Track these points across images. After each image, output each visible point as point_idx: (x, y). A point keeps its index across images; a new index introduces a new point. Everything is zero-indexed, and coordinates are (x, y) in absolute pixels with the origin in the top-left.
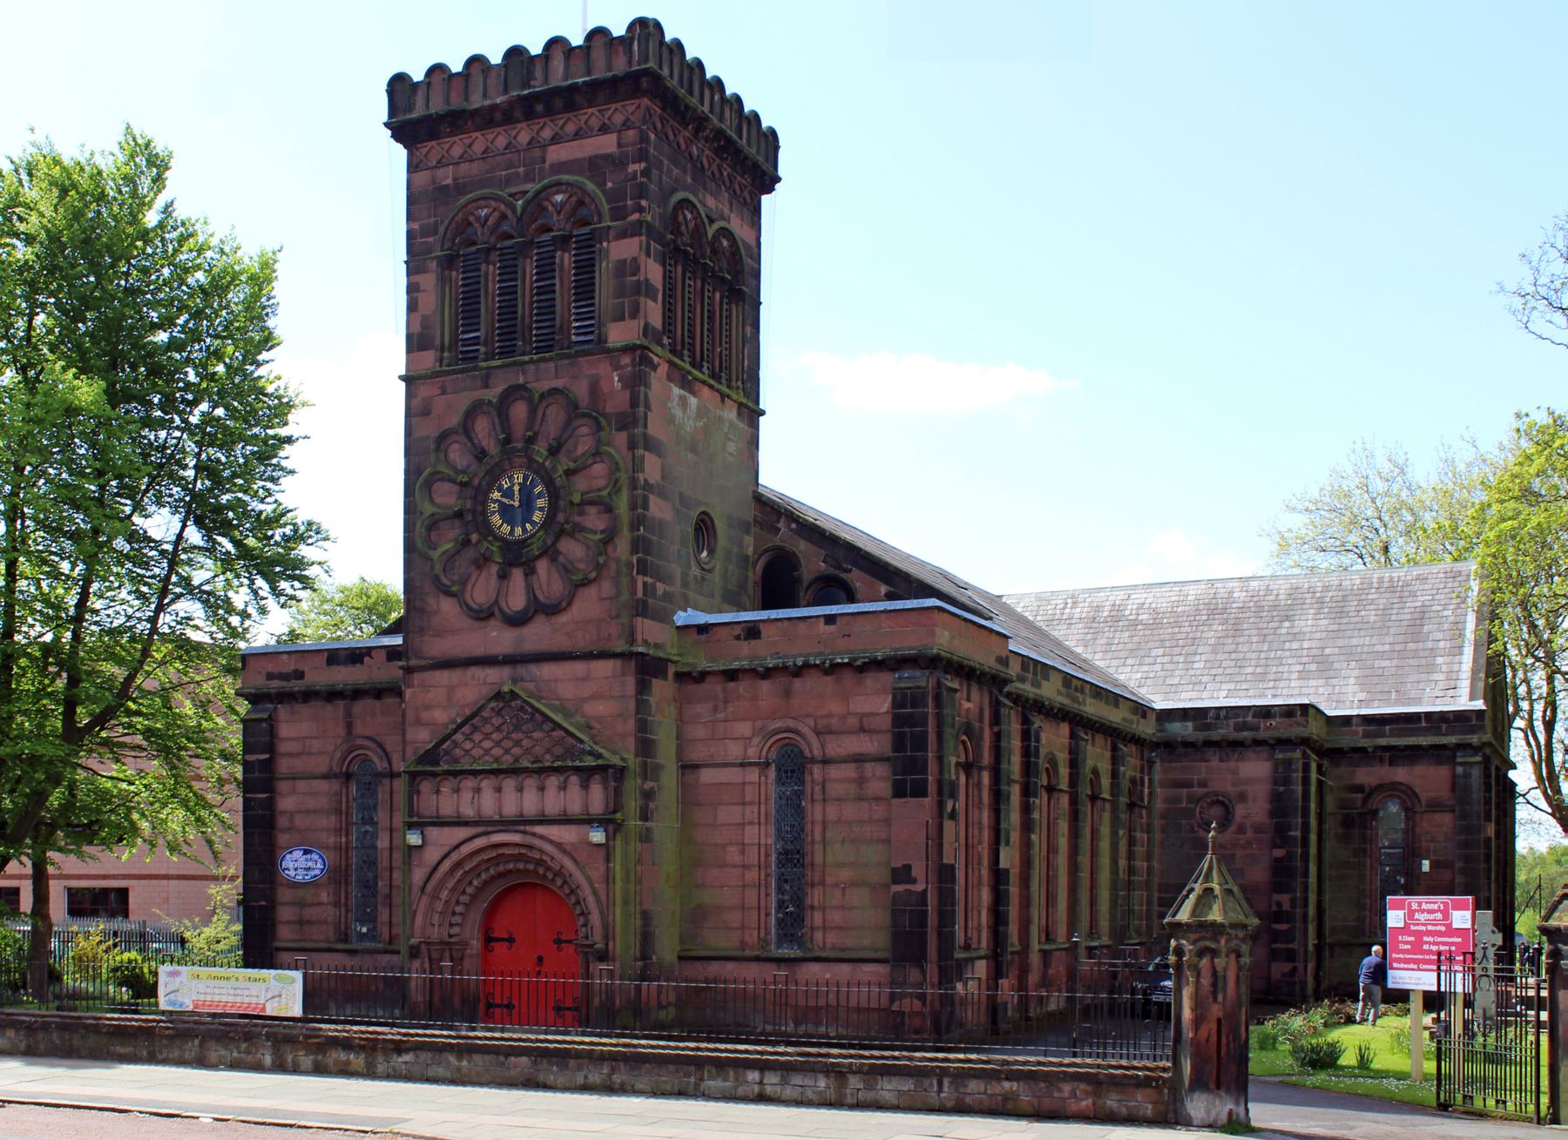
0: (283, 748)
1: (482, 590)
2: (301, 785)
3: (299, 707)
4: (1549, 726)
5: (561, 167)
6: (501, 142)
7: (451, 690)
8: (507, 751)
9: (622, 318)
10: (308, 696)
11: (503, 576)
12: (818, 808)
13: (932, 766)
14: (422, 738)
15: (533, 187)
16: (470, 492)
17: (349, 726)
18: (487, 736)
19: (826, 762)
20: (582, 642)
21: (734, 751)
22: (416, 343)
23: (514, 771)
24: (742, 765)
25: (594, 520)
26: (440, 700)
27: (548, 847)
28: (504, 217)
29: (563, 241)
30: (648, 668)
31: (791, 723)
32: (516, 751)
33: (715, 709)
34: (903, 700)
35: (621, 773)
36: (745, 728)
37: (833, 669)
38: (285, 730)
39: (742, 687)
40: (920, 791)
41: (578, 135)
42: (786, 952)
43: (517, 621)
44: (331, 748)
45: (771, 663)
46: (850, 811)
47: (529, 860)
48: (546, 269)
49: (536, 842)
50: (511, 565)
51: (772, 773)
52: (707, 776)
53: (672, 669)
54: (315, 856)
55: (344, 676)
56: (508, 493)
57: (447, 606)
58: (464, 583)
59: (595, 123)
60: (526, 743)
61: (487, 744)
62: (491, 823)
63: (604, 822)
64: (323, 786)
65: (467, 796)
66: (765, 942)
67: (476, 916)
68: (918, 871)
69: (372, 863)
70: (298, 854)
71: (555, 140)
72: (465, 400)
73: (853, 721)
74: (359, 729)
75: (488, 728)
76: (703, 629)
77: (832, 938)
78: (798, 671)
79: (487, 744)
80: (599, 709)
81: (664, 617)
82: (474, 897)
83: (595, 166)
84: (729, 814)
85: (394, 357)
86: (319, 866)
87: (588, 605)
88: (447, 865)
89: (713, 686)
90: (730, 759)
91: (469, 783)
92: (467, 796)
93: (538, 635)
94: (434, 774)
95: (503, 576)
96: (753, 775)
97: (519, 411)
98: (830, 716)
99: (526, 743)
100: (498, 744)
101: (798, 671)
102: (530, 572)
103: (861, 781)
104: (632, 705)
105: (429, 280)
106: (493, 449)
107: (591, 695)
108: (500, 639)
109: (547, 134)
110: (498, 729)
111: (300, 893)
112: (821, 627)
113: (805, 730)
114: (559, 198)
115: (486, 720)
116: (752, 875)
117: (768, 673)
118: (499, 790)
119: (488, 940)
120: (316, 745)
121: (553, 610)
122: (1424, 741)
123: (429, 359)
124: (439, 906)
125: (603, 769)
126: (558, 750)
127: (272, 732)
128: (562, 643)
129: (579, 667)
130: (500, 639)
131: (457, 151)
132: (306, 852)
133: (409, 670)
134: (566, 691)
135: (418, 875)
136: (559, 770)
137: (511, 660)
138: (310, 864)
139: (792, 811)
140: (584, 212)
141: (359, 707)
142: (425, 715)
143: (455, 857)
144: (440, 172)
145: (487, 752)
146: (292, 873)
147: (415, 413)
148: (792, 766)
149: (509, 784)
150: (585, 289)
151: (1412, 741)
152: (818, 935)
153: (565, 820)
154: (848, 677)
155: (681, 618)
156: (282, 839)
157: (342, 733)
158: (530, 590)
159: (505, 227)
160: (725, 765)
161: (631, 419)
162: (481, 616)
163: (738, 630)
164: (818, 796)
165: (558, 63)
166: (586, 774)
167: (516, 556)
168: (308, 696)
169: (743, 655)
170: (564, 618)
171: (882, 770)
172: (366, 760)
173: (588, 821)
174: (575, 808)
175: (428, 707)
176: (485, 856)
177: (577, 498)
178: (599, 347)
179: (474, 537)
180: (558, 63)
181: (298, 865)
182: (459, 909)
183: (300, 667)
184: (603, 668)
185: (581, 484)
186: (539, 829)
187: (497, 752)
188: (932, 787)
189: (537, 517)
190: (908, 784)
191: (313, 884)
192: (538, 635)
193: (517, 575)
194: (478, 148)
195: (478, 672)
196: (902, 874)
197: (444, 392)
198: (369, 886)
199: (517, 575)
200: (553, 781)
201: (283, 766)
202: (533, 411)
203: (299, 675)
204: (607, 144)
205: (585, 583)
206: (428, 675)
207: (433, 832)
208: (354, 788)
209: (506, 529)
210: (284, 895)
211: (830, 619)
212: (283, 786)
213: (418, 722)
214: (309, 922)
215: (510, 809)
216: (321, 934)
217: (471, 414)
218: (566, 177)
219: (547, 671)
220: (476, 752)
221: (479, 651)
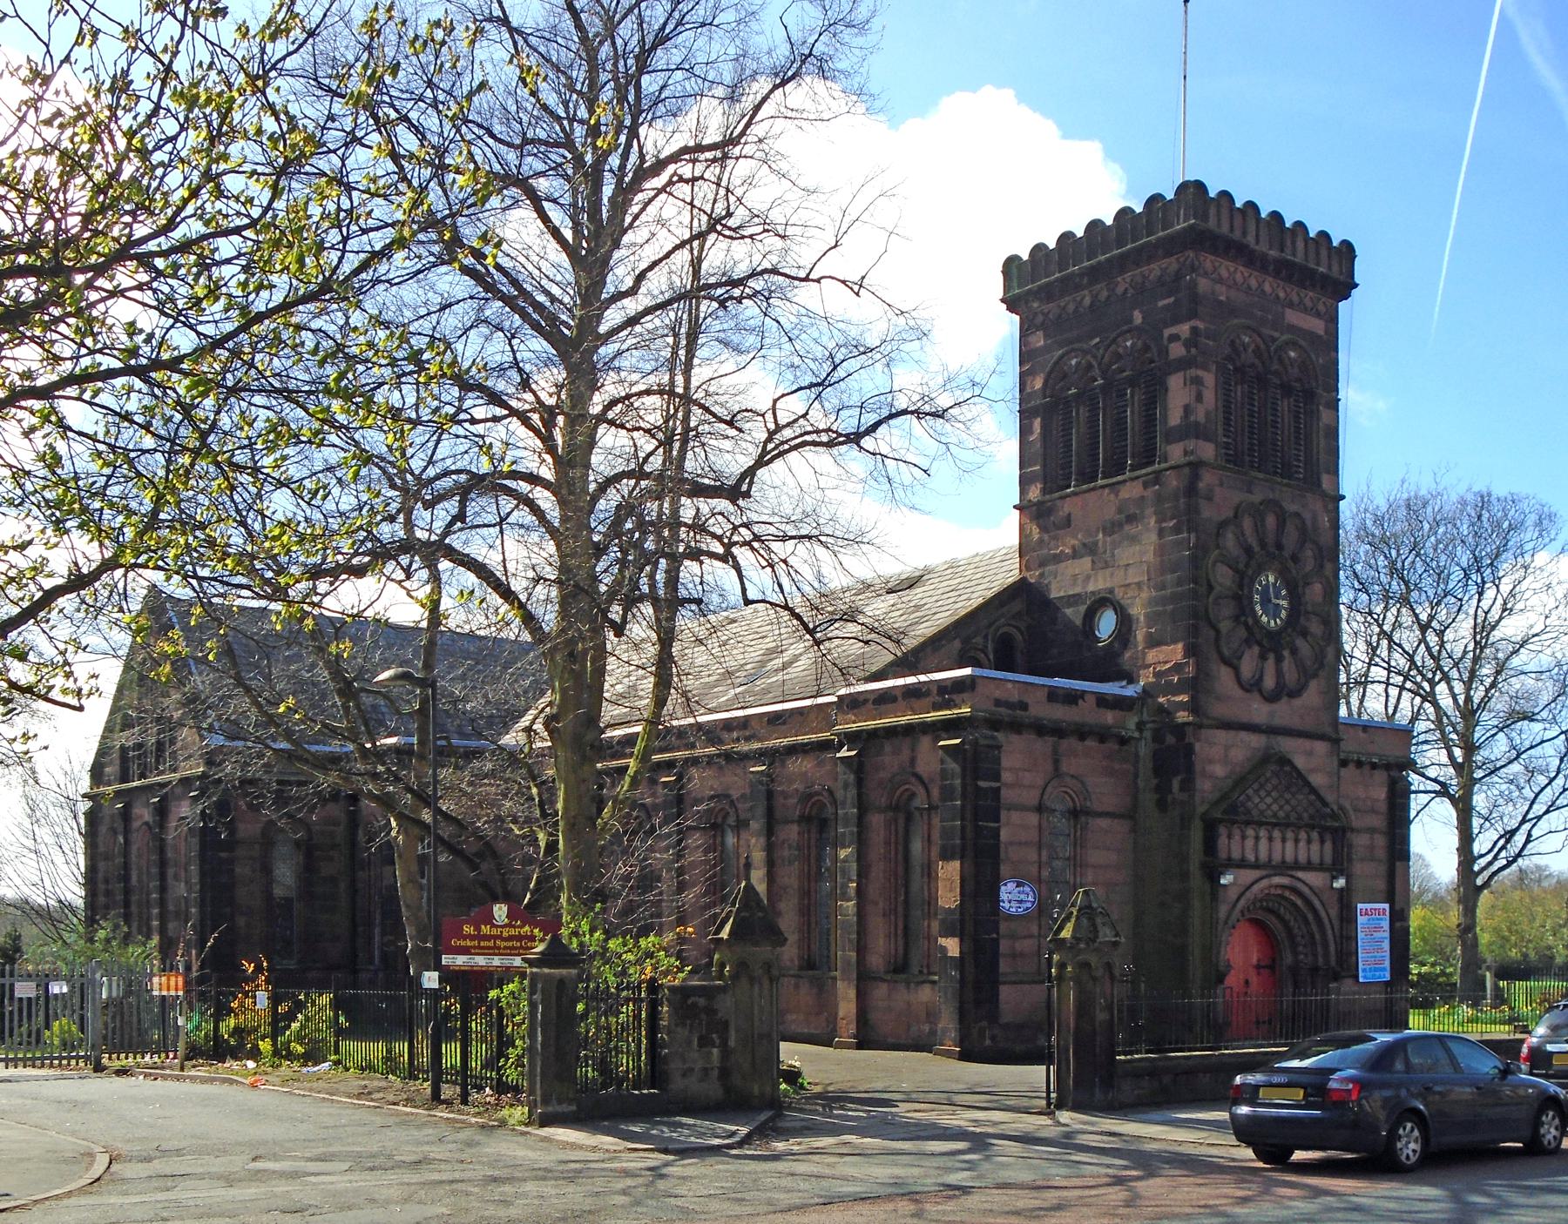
7: (1227, 748)
8: (1281, 807)
17: (1056, 762)
18: (1269, 794)
20: (1308, 724)
23: (1283, 825)
32: (1287, 808)
43: (1272, 698)
44: (1040, 782)
50: (1270, 650)
54: (1027, 889)
57: (1225, 673)
60: (1293, 802)
61: (1269, 800)
70: (1011, 886)
72: (1237, 497)
74: (1064, 768)
87: (1312, 695)
93: (1283, 714)
99: (1293, 802)
100: (1275, 801)
108: (1259, 711)
110: (1275, 788)
114: (1292, 354)
120: (1028, 778)
121: (1294, 694)
130: (1259, 711)
137: (1272, 731)
138: (1022, 897)
141: (1065, 744)
142: (1209, 768)
144: (1218, 287)
145: (1269, 806)
146: (1007, 905)
153: (1309, 867)
156: (1004, 869)
157: (1049, 767)
158: (1279, 673)
162: (1252, 686)
167: (1272, 643)
170: (1297, 702)
177: (1310, 608)
183: (1026, 699)
184: (1321, 747)
186: (1300, 874)
187: (1275, 807)
192: (1283, 714)
195: (1243, 735)
197: (1221, 485)
206: (1211, 732)
209: (1265, 619)
210: (1003, 927)
212: (1003, 814)
214: (1022, 955)
220: (1263, 806)
221: (1245, 719)
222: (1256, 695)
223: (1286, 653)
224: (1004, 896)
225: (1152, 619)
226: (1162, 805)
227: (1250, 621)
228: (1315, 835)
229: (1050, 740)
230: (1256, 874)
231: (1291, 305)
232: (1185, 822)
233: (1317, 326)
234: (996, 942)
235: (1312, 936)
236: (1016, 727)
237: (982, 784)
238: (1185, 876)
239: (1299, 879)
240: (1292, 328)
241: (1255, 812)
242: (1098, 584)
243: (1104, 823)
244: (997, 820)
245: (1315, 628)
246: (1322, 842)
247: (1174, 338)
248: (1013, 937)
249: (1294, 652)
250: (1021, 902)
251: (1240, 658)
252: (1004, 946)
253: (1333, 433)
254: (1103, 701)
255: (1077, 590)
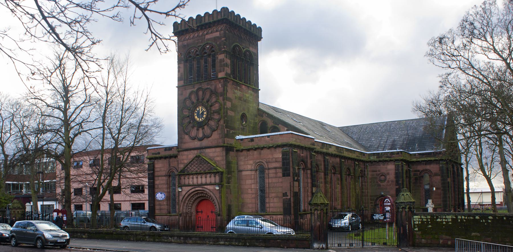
0: (156, 170)
1: (194, 133)
2: (160, 178)
3: (159, 160)
4: (481, 154)
5: (208, 40)
6: (196, 35)
7: (187, 155)
9: (221, 72)
10: (161, 158)
11: (198, 130)
12: (267, 179)
13: (291, 170)
14: (182, 166)
15: (202, 44)
16: (190, 111)
17: (170, 165)
18: (194, 166)
19: (269, 169)
21: (249, 167)
22: (179, 79)
24: (251, 170)
25: (216, 117)
26: (186, 157)
27: (207, 191)
28: (197, 51)
29: (209, 55)
30: (228, 149)
31: (261, 160)
32: (201, 169)
33: (245, 158)
34: (284, 154)
35: (222, 173)
36: (251, 162)
37: (269, 148)
38: (156, 166)
39: (251, 153)
40: (288, 175)
41: (211, 33)
42: (262, 213)
43: (201, 140)
45: (256, 147)
46: (274, 180)
47: (204, 194)
48: (206, 62)
49: (205, 189)
51: (258, 172)
52: (244, 173)
53: (235, 149)
55: (168, 153)
56: (199, 111)
57: (187, 137)
58: (190, 132)
59: (215, 30)
61: (194, 168)
62: (196, 185)
63: (218, 185)
64: (164, 178)
65: (191, 179)
66: (257, 212)
67: (194, 206)
68: (288, 194)
69: (174, 195)
70: (159, 194)
71: (207, 34)
72: (189, 91)
73: (274, 160)
74: (172, 165)
75: (195, 164)
76: (242, 140)
77: (271, 210)
78: (263, 148)
79: (194, 168)
80: (218, 159)
81: (233, 138)
82: (193, 202)
83: (215, 39)
84: (249, 182)
85: (175, 83)
87: (215, 135)
88: (187, 195)
89: (245, 153)
90: (249, 169)
91: (191, 176)
92: (191, 179)
93: (205, 143)
94: (184, 175)
95: (198, 130)
96: (253, 173)
97: (200, 93)
98: (269, 158)
100: (197, 167)
101: (263, 148)
102: (203, 129)
103: (276, 173)
104: (225, 157)
105: (182, 66)
106: (195, 101)
107: (216, 156)
108: (197, 144)
109: (205, 33)
110: (197, 164)
111: (160, 202)
112: (267, 138)
113: (264, 162)
115: (194, 162)
116: (254, 196)
117: (256, 149)
118: (197, 178)
119: (197, 212)
121: (208, 137)
122: (432, 159)
123: (182, 82)
124: (186, 204)
125: (218, 172)
126: (209, 168)
127: (154, 167)
128: (210, 144)
129: (213, 150)
130: (197, 144)
131: (187, 37)
133: (179, 151)
134: (211, 155)
135: (181, 198)
136: (210, 173)
139: (262, 179)
140: (213, 49)
141: (171, 160)
142: (182, 162)
143: (188, 193)
147: (179, 95)
148: (261, 170)
149: (199, 176)
150: (214, 66)
151: (429, 159)
152: (268, 209)
153: (211, 184)
154: (273, 149)
155: (238, 137)
156: (156, 190)
157: (168, 166)
158: (203, 133)
159: (197, 53)
160: (247, 171)
161: (224, 94)
162: (194, 139)
163: (249, 140)
164: (267, 177)
165: (207, 17)
166: (215, 173)
167: (200, 125)
168: (161, 158)
169: (251, 145)
170: (210, 138)
171: (280, 171)
172: (173, 172)
173: (215, 184)
174: (213, 182)
175: (183, 160)
176: (195, 193)
178: (217, 78)
179: (192, 121)
180: (207, 17)
181: (160, 196)
182: (190, 205)
184: (218, 149)
185: (213, 109)
186: (205, 187)
188: (291, 174)
189: (204, 116)
190: (286, 174)
192: (205, 143)
193: (201, 129)
194: (192, 36)
195: (192, 151)
196: (285, 194)
198: (174, 200)
199: (201, 129)
200: (208, 176)
201: (156, 174)
202: (203, 93)
203: (159, 153)
204: (217, 34)
205: (214, 131)
206: (182, 152)
207: (184, 188)
208: (171, 179)
209: (198, 119)
210: (157, 203)
211: (268, 136)
212: (156, 178)
213: (181, 163)
215: (200, 182)
216: (165, 212)
217: (191, 94)
218: (209, 42)
219: (208, 150)
229: (168, 159)
230: (190, 188)
236: (156, 158)
241: (190, 171)
248: (160, 205)
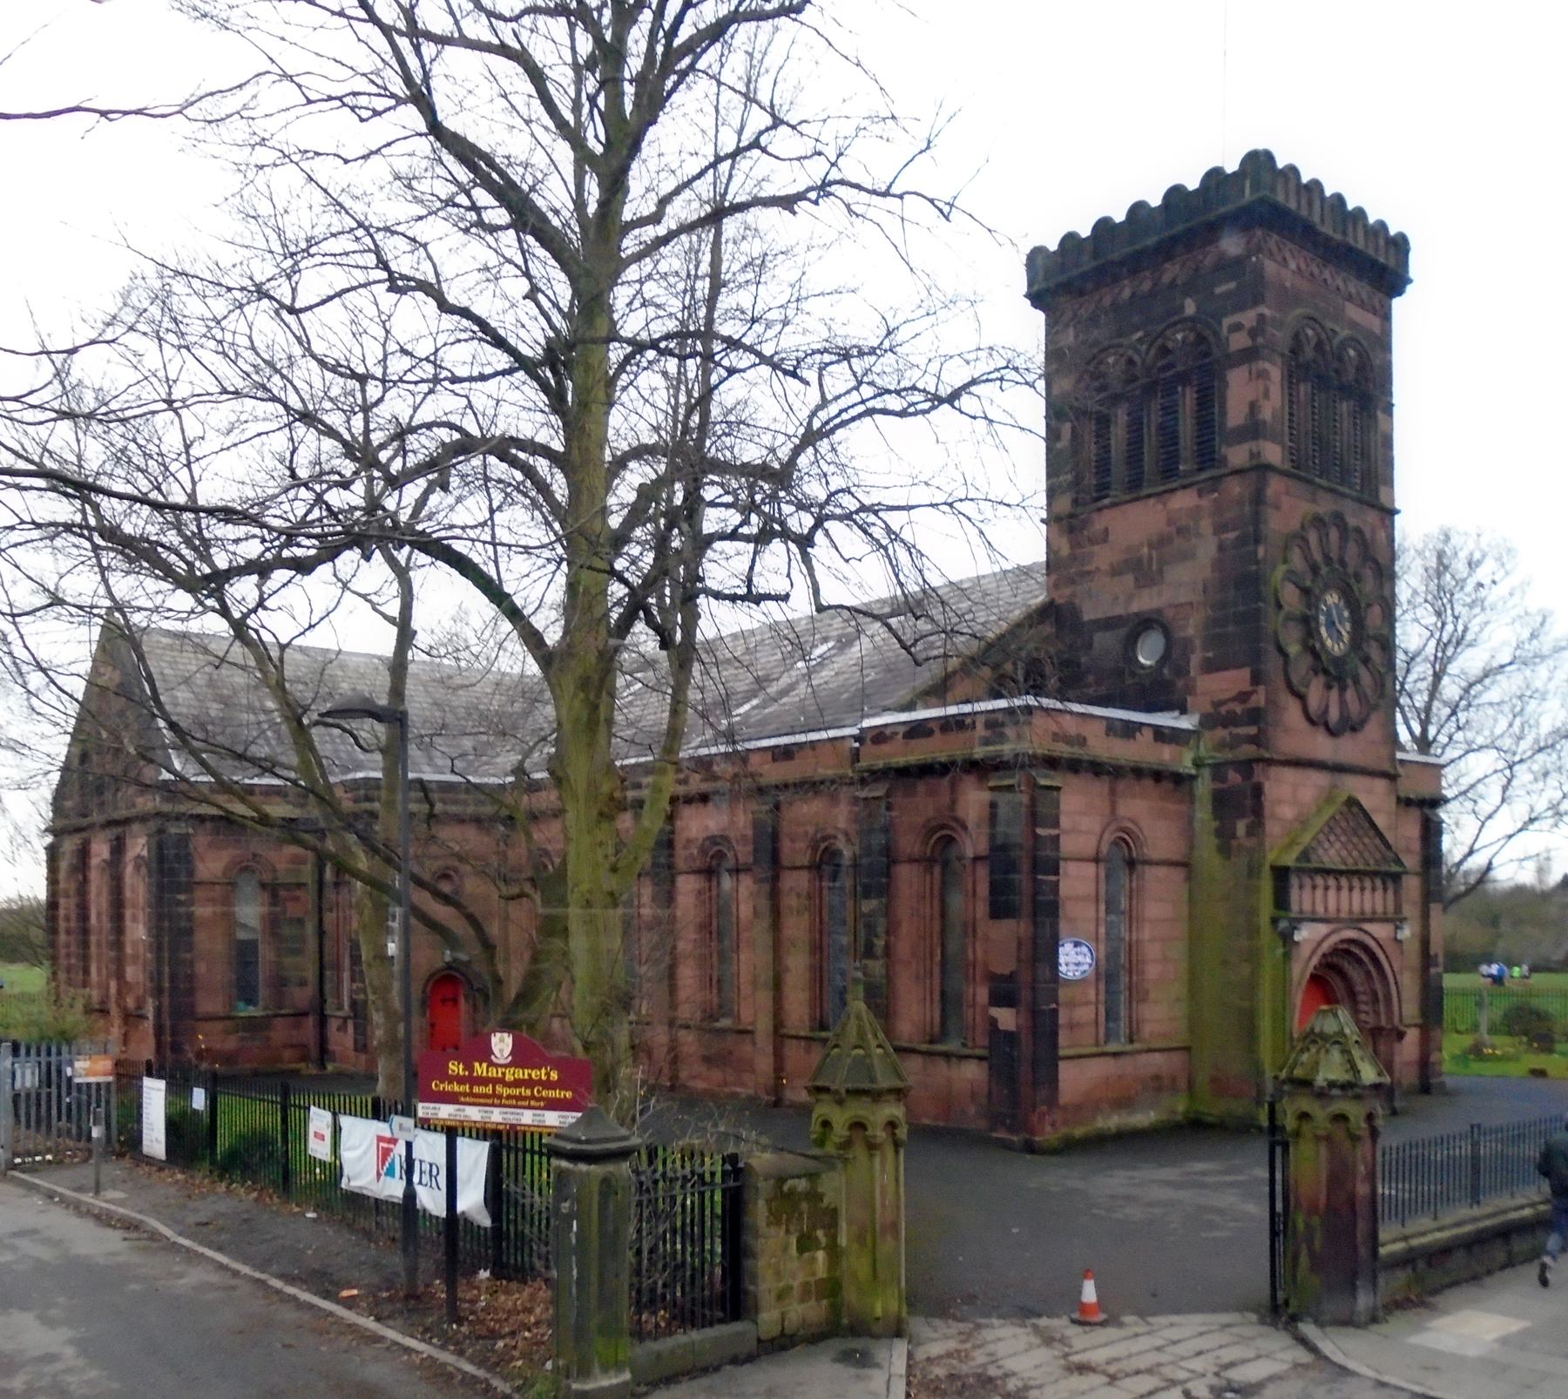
27: (1372, 944)
44: (1097, 828)
54: (1085, 949)
86: (1088, 960)
108: (1322, 746)
130: (1322, 746)
132: (1076, 944)
138: (1080, 958)
158: (1343, 703)
184: (1380, 785)
186: (1367, 926)
191: (1082, 982)
197: (1287, 493)
210: (1063, 994)
222: (1322, 729)
223: (1349, 682)
224: (1062, 959)
225: (1212, 641)
226: (1225, 850)
227: (1318, 646)
228: (1378, 882)
231: (1350, 298)
232: (1253, 871)
233: (1375, 323)
234: (1055, 1011)
235: (1375, 994)
237: (1039, 831)
238: (1253, 931)
239: (1366, 932)
240: (1354, 325)
242: (1145, 602)
243: (1162, 871)
244: (1057, 873)
245: (1375, 653)
246: (1385, 889)
247: (1237, 327)
249: (1356, 681)
250: (1078, 964)
251: (1307, 686)
252: (1063, 1018)
253: (1388, 442)
254: (1160, 734)
255: (1119, 610)
